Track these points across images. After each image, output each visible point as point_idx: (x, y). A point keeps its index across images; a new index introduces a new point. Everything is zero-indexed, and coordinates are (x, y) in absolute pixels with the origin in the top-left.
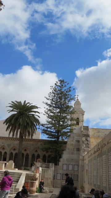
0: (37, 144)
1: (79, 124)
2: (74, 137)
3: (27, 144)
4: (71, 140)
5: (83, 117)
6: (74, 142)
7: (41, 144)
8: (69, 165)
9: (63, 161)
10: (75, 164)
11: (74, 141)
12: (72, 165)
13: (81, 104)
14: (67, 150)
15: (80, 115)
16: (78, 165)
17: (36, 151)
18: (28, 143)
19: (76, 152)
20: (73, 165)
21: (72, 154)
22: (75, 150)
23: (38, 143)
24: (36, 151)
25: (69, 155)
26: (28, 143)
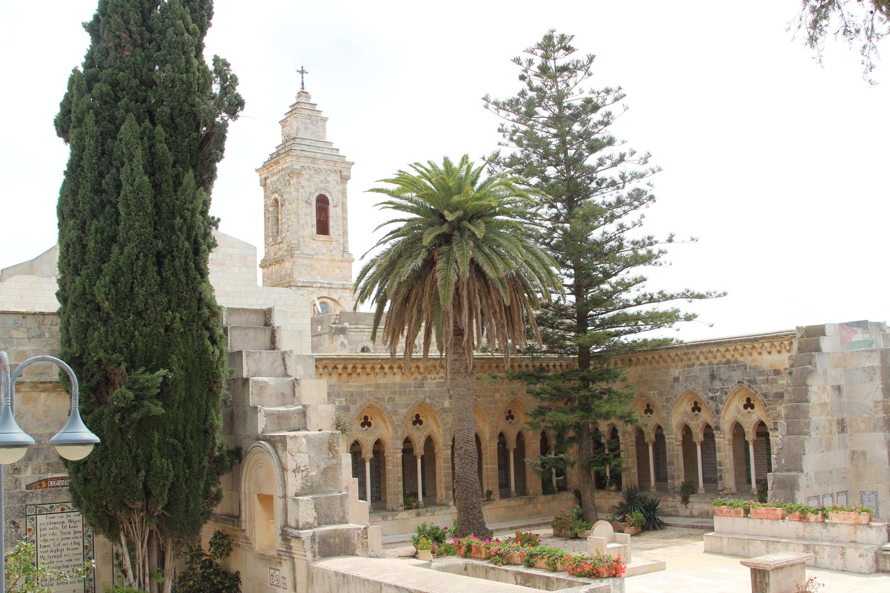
0: (421, 386)
1: (331, 230)
2: (825, 373)
3: (378, 386)
4: (819, 387)
5: (344, 193)
6: (827, 397)
7: (439, 385)
8: (824, 496)
9: (808, 487)
10: (837, 488)
11: (829, 389)
12: (832, 495)
13: (325, 120)
14: (813, 434)
15: (333, 178)
16: (846, 492)
17: (417, 421)
18: (382, 381)
19: (837, 435)
20: (835, 495)
21: (829, 448)
22: (835, 428)
23: (424, 378)
24: (417, 421)
25: (819, 455)
26: (382, 381)
